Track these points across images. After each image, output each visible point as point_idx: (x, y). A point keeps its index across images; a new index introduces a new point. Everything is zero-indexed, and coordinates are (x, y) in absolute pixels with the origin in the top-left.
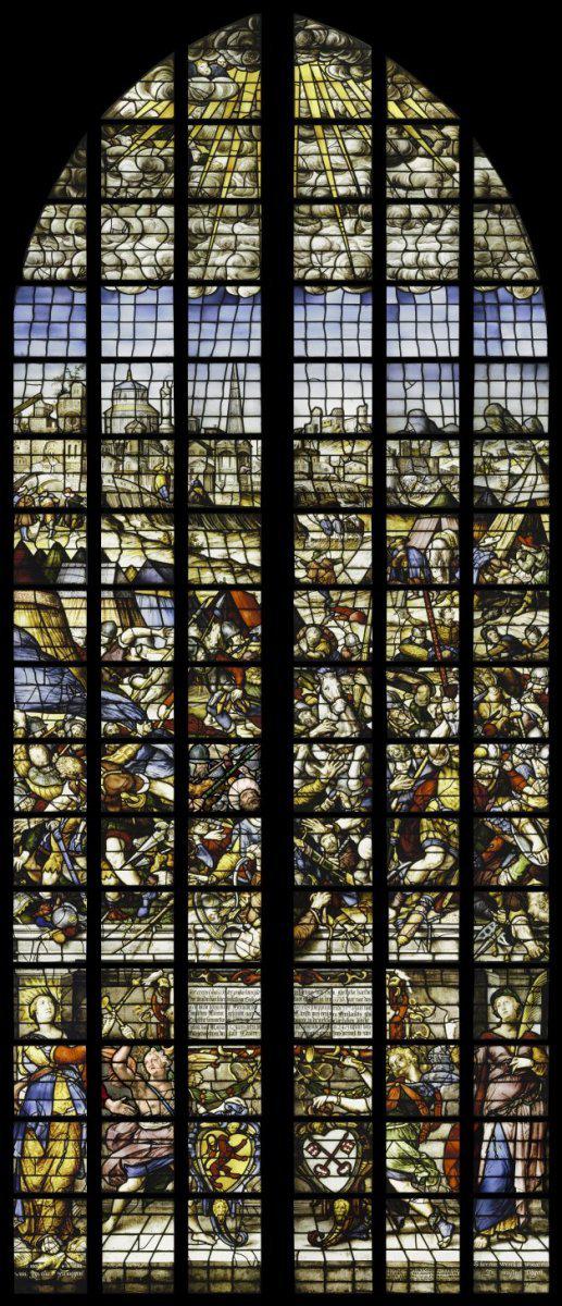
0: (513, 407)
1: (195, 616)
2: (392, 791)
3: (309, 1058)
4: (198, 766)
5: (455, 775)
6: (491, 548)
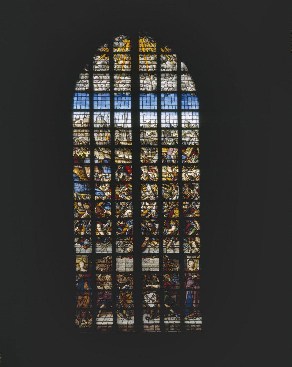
0: (191, 121)
3: (145, 276)
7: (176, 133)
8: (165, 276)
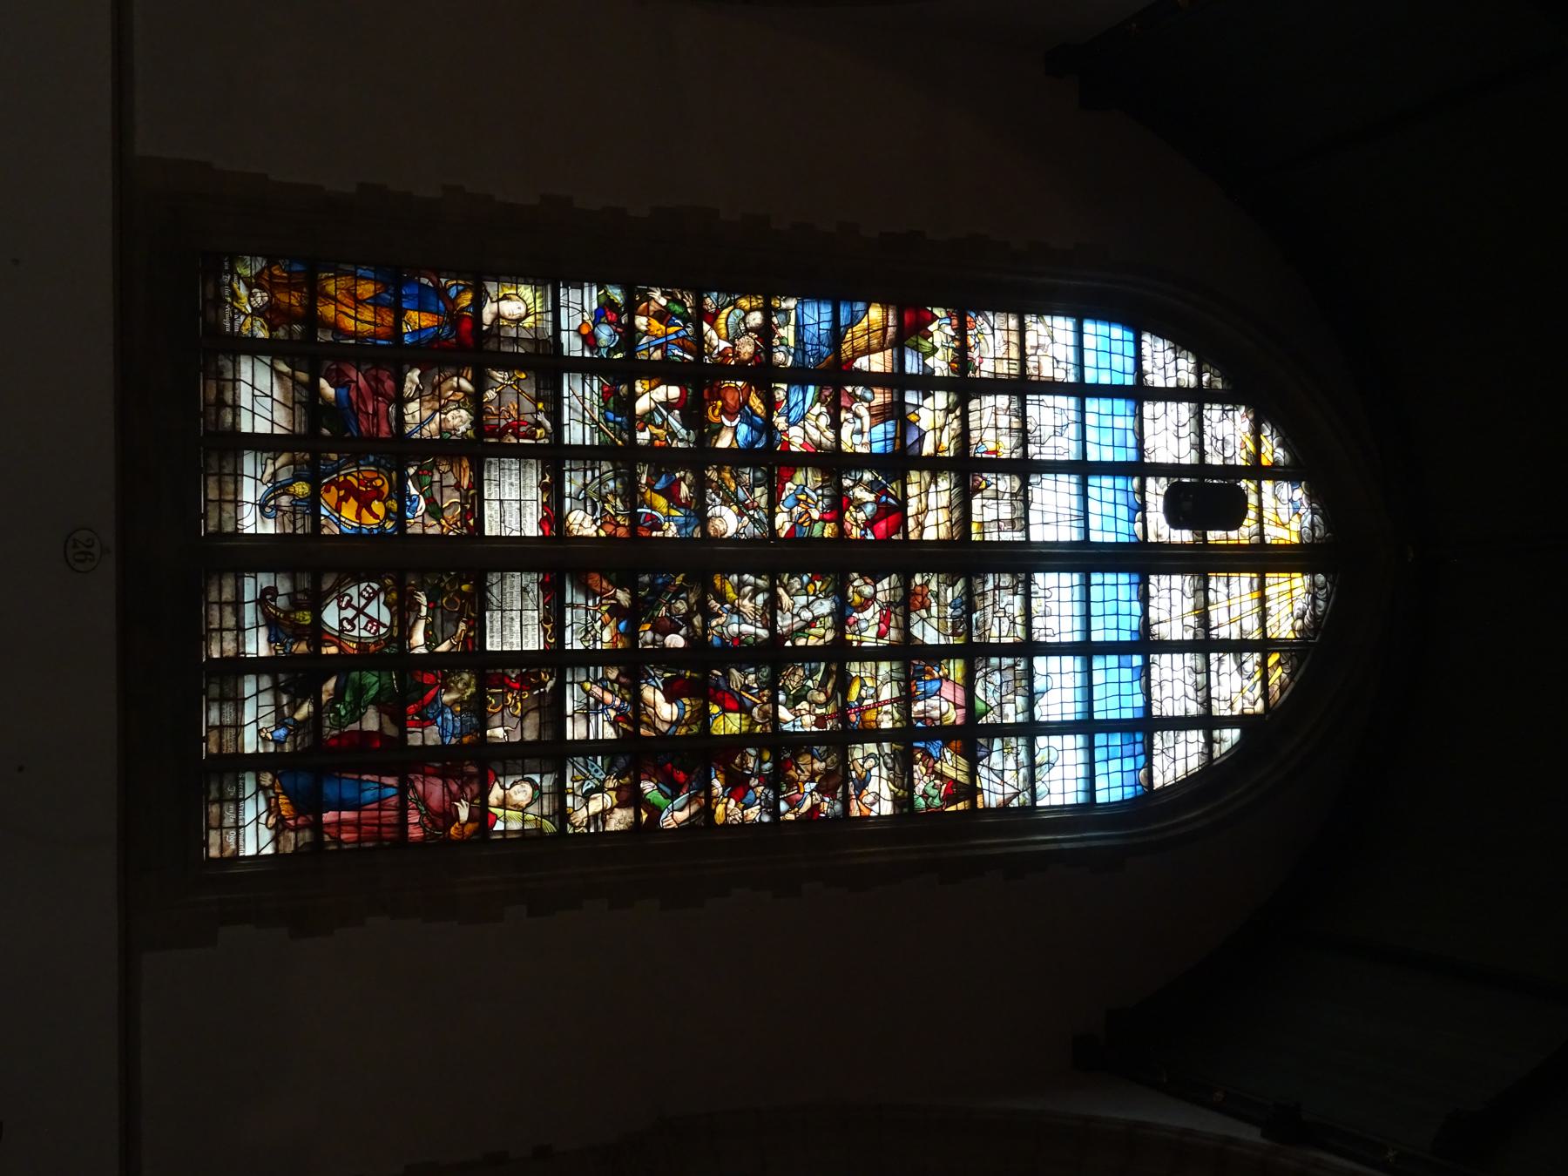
0: (1056, 772)
1: (880, 478)
2: (728, 670)
3: (465, 587)
4: (747, 476)
5: (744, 729)
6: (943, 758)
7: (1016, 713)
8: (466, 676)
